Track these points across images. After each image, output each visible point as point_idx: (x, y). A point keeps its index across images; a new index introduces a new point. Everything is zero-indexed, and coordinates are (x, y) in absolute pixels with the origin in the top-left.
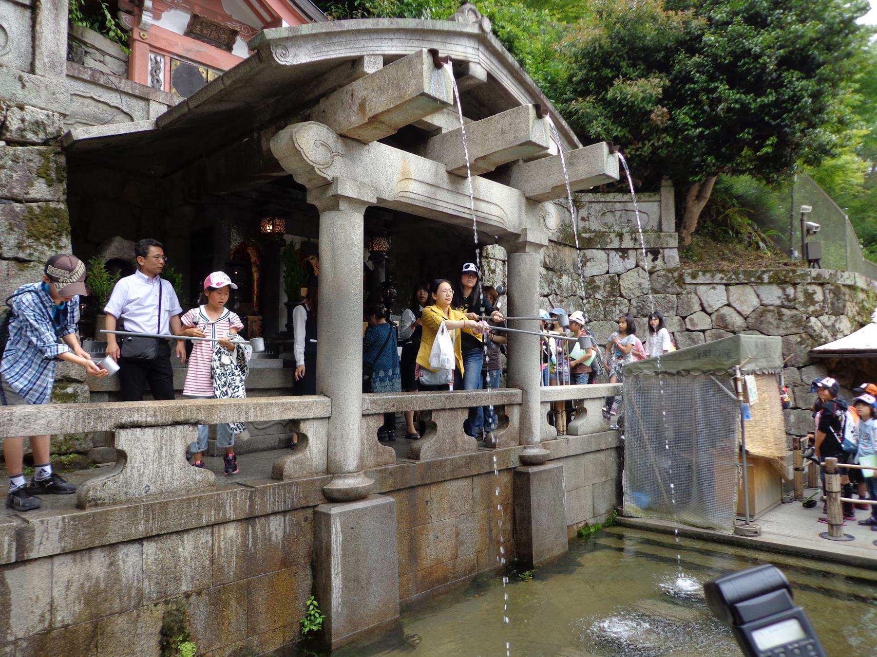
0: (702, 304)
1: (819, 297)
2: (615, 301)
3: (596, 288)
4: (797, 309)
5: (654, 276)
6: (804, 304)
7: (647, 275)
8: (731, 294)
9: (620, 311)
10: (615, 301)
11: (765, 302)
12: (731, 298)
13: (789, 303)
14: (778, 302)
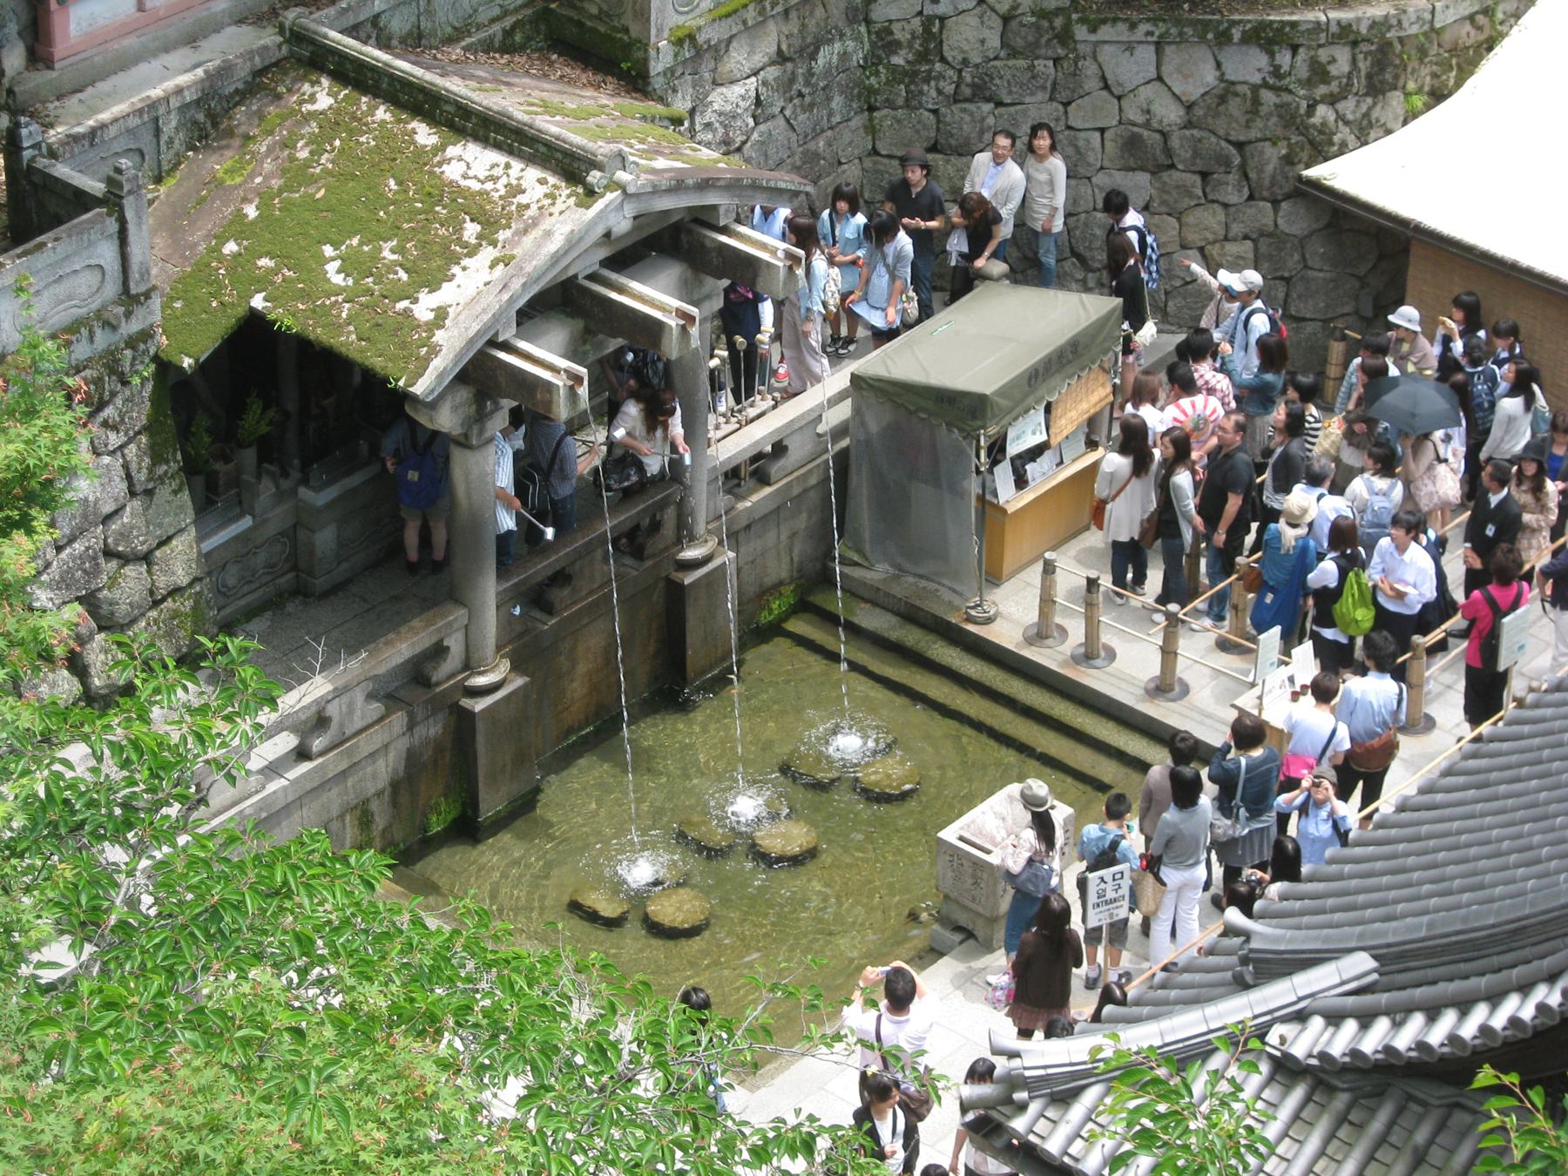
0: (1104, 78)
1: (1341, 66)
2: (930, 71)
3: (894, 47)
4: (1290, 92)
5: (1014, 24)
6: (1308, 83)
7: (997, 23)
8: (1166, 59)
9: (939, 92)
10: (930, 71)
11: (1230, 76)
12: (1165, 70)
13: (1277, 80)
14: (1256, 79)
